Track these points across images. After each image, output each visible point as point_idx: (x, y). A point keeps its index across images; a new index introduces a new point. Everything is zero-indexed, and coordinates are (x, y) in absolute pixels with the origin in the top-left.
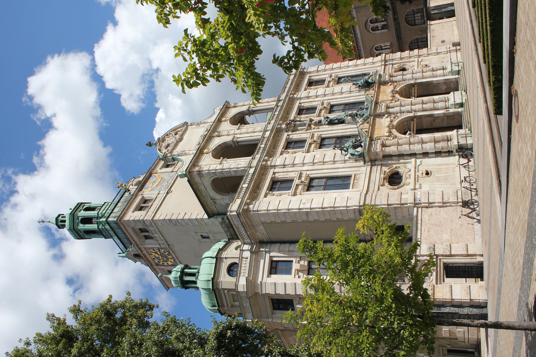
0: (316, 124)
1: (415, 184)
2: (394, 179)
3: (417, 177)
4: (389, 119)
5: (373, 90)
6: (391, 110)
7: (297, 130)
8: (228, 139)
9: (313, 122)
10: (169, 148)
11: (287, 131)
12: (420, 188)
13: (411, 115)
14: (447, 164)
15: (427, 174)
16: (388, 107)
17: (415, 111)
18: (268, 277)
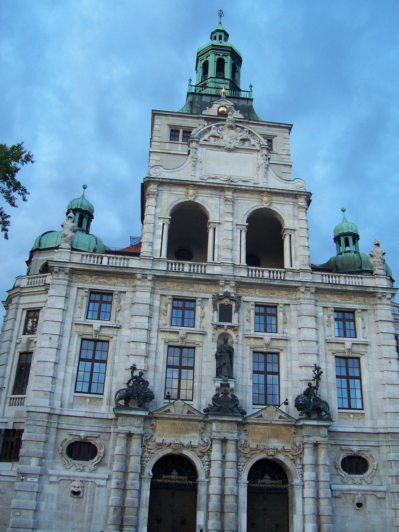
0: (221, 336)
1: (58, 476)
2: (81, 450)
3: (71, 479)
4: (195, 442)
5: (280, 417)
6: (216, 447)
7: (215, 309)
8: (213, 217)
9: (230, 332)
10: (212, 139)
11: (214, 295)
12: (51, 482)
13: (202, 477)
14: (90, 520)
15: (76, 493)
16: (224, 441)
17: (209, 482)
18: (23, 309)
